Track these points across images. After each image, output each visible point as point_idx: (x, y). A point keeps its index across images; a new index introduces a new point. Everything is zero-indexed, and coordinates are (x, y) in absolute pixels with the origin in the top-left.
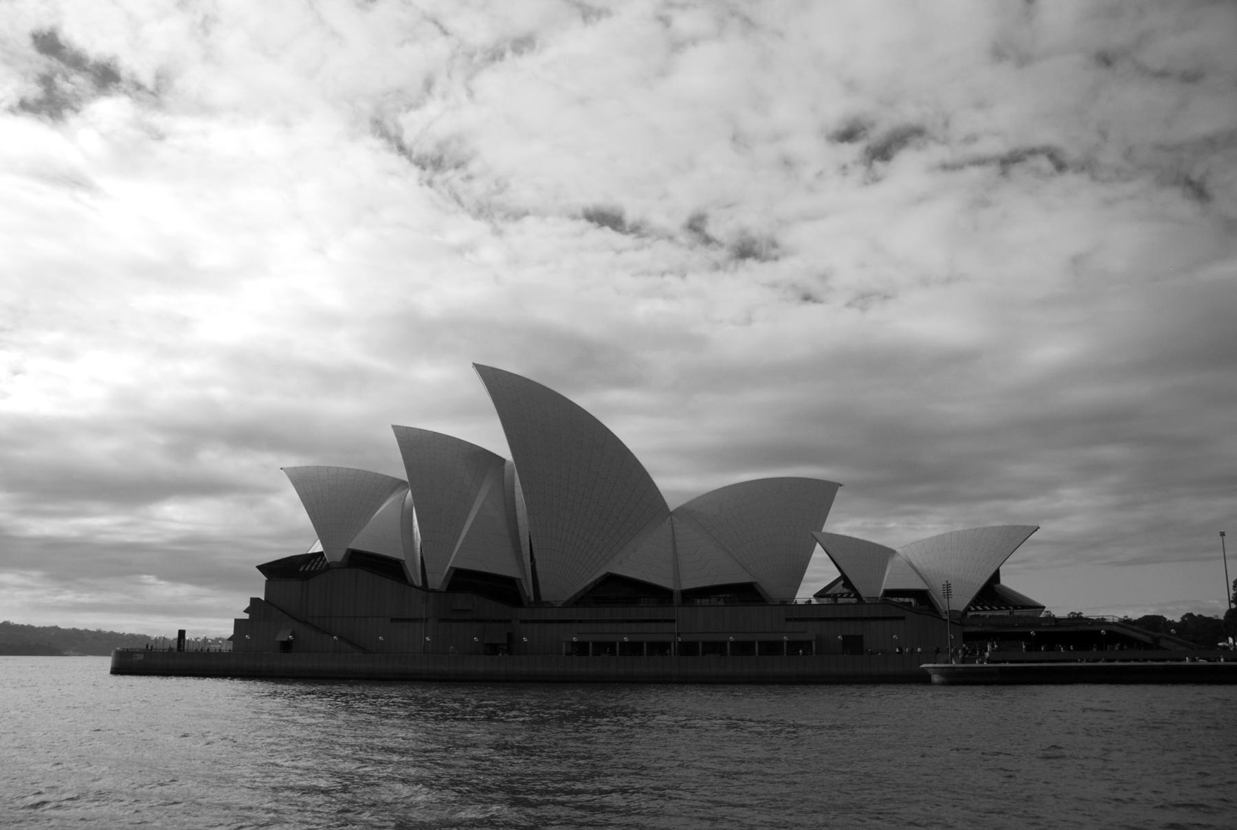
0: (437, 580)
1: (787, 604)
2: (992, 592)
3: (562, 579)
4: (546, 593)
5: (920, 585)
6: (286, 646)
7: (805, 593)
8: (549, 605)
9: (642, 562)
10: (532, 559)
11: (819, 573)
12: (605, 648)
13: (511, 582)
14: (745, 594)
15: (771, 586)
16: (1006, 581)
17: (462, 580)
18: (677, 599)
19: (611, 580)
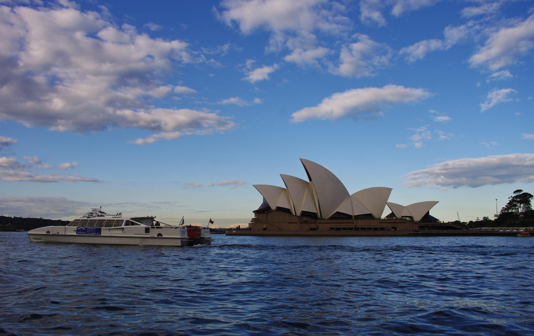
0: (299, 214)
1: (380, 219)
2: (427, 217)
3: (328, 214)
4: (323, 216)
5: (410, 215)
6: (265, 229)
7: (384, 216)
8: (324, 219)
9: (343, 208)
10: (320, 208)
11: (386, 212)
12: (338, 229)
13: (315, 214)
14: (369, 216)
15: (375, 215)
16: (430, 214)
17: (304, 214)
18: (353, 217)
19: (338, 213)
